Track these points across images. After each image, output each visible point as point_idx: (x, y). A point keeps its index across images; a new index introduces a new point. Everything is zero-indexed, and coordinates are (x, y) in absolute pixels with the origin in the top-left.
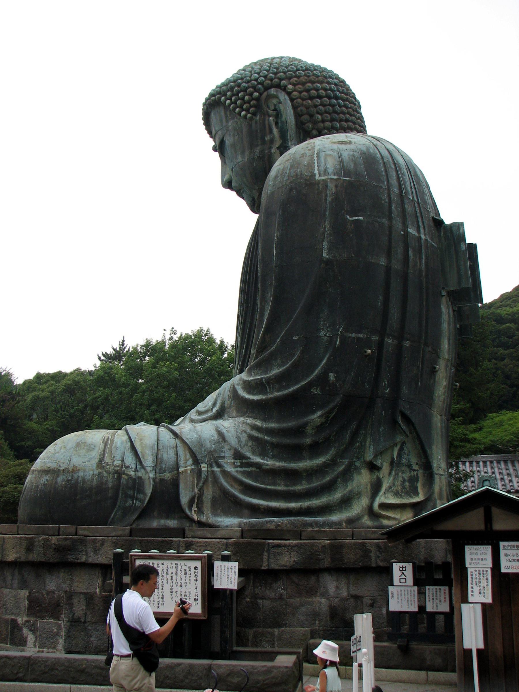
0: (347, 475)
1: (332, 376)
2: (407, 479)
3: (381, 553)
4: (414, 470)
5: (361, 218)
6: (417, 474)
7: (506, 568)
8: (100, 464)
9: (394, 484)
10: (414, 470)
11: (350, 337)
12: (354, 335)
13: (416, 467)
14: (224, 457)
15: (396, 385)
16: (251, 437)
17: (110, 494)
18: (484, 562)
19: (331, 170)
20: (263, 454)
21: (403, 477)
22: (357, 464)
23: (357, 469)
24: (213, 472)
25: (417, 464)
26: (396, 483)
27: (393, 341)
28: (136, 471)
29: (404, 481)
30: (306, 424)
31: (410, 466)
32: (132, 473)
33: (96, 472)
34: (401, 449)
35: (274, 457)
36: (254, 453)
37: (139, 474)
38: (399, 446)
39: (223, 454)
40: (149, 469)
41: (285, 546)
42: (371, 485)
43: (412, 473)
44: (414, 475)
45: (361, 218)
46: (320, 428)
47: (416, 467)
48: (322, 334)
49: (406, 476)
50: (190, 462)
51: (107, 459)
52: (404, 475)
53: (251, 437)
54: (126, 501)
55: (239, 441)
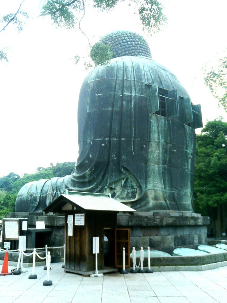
1: (91, 156)
5: (101, 94)
6: (136, 190)
7: (76, 223)
8: (28, 193)
10: (135, 189)
11: (96, 140)
12: (98, 139)
13: (135, 187)
14: (62, 188)
15: (119, 156)
16: (72, 180)
17: (29, 202)
18: (71, 221)
19: (92, 78)
20: (74, 186)
21: (128, 192)
22: (106, 187)
23: (105, 189)
24: (58, 193)
25: (136, 186)
26: (123, 194)
27: (116, 139)
28: (35, 194)
29: (128, 193)
30: (85, 174)
31: (132, 187)
32: (34, 195)
33: (26, 195)
34: (127, 180)
35: (78, 187)
36: (71, 186)
37: (36, 195)
38: (125, 180)
39: (62, 187)
40: (39, 193)
41: (61, 218)
43: (134, 190)
45: (101, 94)
46: (90, 175)
47: (135, 187)
48: (88, 140)
49: (130, 191)
50: (52, 190)
51: (30, 191)
52: (128, 191)
53: (72, 180)
54: (32, 204)
55: (68, 182)
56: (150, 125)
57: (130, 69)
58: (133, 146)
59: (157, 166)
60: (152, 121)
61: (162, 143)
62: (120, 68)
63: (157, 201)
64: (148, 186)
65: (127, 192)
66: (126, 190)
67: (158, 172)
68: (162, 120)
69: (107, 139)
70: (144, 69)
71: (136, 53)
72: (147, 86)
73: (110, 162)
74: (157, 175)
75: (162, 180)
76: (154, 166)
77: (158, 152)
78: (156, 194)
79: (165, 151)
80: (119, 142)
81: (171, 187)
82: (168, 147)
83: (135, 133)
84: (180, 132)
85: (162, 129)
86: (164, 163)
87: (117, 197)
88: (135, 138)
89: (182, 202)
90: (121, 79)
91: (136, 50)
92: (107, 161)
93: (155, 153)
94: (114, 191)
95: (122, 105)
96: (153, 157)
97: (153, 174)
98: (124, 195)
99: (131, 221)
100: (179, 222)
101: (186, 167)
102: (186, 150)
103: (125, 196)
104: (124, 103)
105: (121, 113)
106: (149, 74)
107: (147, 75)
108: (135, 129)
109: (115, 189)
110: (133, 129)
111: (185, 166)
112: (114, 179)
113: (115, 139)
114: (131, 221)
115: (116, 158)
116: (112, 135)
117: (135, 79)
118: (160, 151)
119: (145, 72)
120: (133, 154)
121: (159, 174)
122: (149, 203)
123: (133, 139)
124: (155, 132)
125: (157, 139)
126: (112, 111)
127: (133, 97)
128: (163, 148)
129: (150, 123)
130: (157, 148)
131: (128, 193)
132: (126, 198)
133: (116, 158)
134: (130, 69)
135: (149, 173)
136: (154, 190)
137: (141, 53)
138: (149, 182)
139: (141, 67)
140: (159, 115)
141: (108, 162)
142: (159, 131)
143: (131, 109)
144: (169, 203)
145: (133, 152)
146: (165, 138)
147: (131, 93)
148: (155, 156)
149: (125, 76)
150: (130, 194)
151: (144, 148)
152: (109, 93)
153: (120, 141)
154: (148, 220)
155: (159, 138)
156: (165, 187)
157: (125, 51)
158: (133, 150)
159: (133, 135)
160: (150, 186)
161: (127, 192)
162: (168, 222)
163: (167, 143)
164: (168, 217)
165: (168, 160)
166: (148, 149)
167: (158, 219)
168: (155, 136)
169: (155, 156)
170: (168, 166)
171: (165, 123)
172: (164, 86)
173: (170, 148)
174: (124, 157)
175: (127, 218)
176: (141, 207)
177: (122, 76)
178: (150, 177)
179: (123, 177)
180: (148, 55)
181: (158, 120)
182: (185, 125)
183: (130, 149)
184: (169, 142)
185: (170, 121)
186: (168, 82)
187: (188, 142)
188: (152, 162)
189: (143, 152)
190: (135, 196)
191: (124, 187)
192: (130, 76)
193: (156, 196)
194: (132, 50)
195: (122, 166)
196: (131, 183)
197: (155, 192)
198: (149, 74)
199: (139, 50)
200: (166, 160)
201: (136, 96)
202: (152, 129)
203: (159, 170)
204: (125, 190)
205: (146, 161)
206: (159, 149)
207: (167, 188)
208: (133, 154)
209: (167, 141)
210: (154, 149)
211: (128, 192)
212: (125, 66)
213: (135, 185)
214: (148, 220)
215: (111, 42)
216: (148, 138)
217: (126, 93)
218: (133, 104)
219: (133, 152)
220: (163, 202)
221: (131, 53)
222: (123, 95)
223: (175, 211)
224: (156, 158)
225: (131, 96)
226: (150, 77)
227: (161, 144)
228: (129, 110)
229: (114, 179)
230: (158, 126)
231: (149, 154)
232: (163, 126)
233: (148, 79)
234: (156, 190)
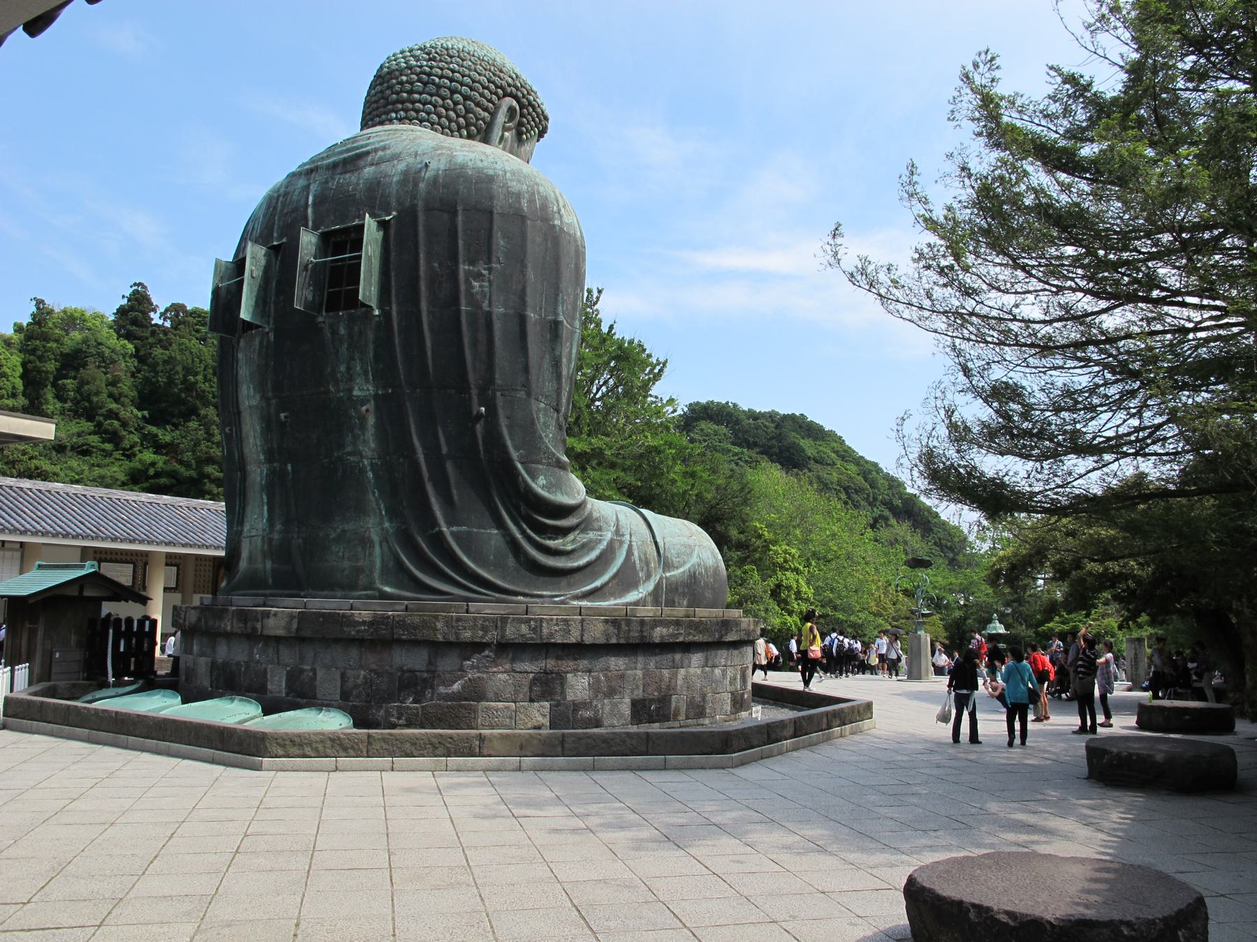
79: (269, 423)
82: (272, 410)
100: (206, 622)
101: (349, 449)
111: (341, 446)
144: (273, 570)
160: (246, 528)
163: (268, 399)
171: (261, 343)
207: (278, 527)
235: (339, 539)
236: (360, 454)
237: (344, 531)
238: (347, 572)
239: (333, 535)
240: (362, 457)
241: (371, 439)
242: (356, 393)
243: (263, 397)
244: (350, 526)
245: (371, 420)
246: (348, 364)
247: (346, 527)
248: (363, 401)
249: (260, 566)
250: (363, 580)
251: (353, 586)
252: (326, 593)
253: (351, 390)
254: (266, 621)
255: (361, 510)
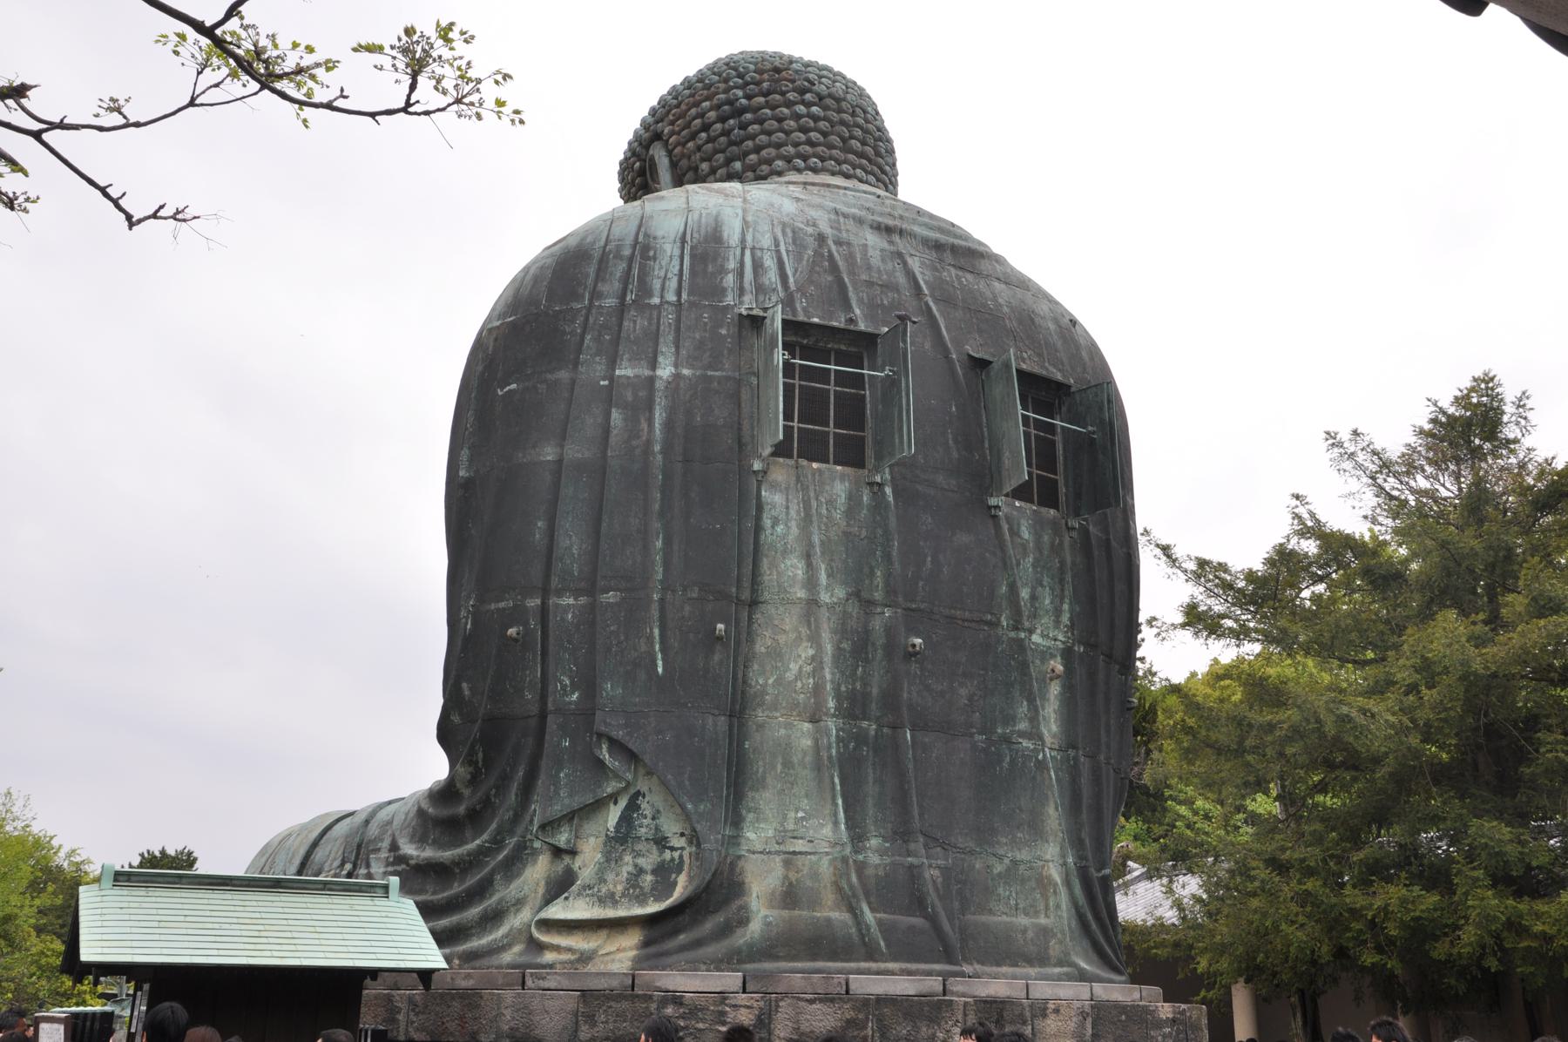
0: (513, 865)
2: (649, 868)
3: (417, 1014)
4: (672, 849)
5: (514, 386)
6: (681, 857)
9: (602, 881)
10: (672, 849)
15: (589, 686)
21: (636, 866)
23: (535, 853)
25: (682, 835)
26: (610, 877)
31: (661, 842)
34: (633, 806)
36: (412, 841)
38: (623, 803)
42: (547, 884)
43: (668, 855)
44: (673, 859)
45: (514, 386)
49: (647, 862)
52: (641, 861)
56: (758, 518)
57: (668, 247)
58: (656, 632)
59: (807, 726)
60: (773, 499)
61: (831, 607)
62: (619, 248)
63: (797, 912)
64: (750, 835)
65: (630, 868)
66: (628, 858)
67: (808, 759)
68: (838, 483)
69: (534, 602)
70: (743, 234)
71: (779, 163)
72: (747, 323)
73: (550, 718)
74: (806, 774)
75: (840, 802)
76: (788, 726)
77: (811, 652)
78: (793, 876)
79: (856, 648)
80: (590, 615)
81: (901, 834)
82: (877, 624)
83: (667, 564)
84: (963, 538)
85: (832, 534)
86: (853, 706)
87: (579, 895)
88: (666, 587)
89: (984, 918)
90: (610, 302)
91: (778, 146)
92: (534, 709)
93: (796, 658)
94: (567, 859)
95: (606, 430)
96: (779, 681)
97: (779, 767)
98: (616, 882)
99: (591, 1019)
101: (1023, 726)
102: (1013, 634)
103: (620, 888)
104: (616, 415)
105: (599, 470)
106: (769, 262)
107: (758, 266)
108: (668, 542)
109: (573, 853)
110: (659, 544)
111: (1010, 719)
112: (567, 801)
113: (571, 601)
114: (591, 1019)
115: (575, 697)
116: (555, 582)
117: (684, 296)
118: (819, 648)
119: (748, 253)
120: (660, 670)
121: (818, 767)
122: (744, 921)
123: (655, 597)
124: (785, 553)
125: (803, 587)
126: (560, 461)
127: (659, 385)
128: (842, 631)
129: (760, 508)
130: (804, 631)
131: (641, 871)
132: (623, 895)
133: (575, 697)
134: (670, 249)
135: (760, 767)
136: (778, 853)
137: (805, 158)
138: (756, 810)
139: (732, 233)
140: (815, 465)
141: (543, 716)
142: (810, 545)
143: (649, 443)
144: (880, 923)
145: (660, 663)
146: (856, 578)
147: (653, 365)
148: (790, 676)
149: (633, 285)
150: (649, 878)
151: (720, 638)
152: (549, 376)
153: (592, 607)
154: (682, 1017)
155: (811, 583)
156: (857, 837)
157: (728, 162)
158: (662, 651)
159: (660, 577)
160: (756, 835)
161: (630, 868)
162: (805, 1027)
163: (867, 605)
164: (811, 1002)
165: (875, 691)
166: (751, 639)
167: (743, 1010)
168: (787, 572)
169: (790, 676)
170: (880, 726)
171: (853, 498)
172: (858, 311)
173: (889, 631)
174: (610, 689)
175: (572, 1006)
176: (698, 943)
177: (617, 285)
178: (761, 784)
179: (609, 790)
180: (845, 167)
181: (805, 489)
182: (993, 501)
183: (643, 648)
184: (878, 596)
185: (888, 490)
186: (898, 291)
187: (1025, 593)
188: (775, 706)
189: (717, 657)
190: (675, 884)
191: (623, 836)
192: (657, 285)
193: (791, 884)
194: (758, 149)
195: (600, 735)
196: (653, 818)
197: (787, 864)
198: (769, 262)
199: (796, 145)
200: (866, 696)
201: (677, 376)
202: (767, 536)
203: (817, 748)
204: (621, 858)
205: (738, 706)
206: (815, 639)
207: (874, 842)
208: (660, 670)
209: (864, 595)
210: (782, 639)
211: (636, 866)
212: (641, 238)
213: (677, 828)
214: (682, 1017)
215: (672, 123)
216: (746, 584)
217: (624, 371)
218: (659, 416)
219: (660, 663)
220: (839, 916)
221: (753, 168)
222: (611, 379)
223: (913, 966)
224: (799, 684)
225: (651, 380)
226: (772, 276)
227: (824, 614)
228: (638, 451)
229: (565, 802)
230: (807, 520)
231: (756, 667)
232: (838, 515)
233: (760, 289)
234: (794, 853)
235: (1010, 875)
236: (1041, 738)
237: (1015, 862)
238: (1030, 934)
239: (999, 868)
240: (1043, 744)
241: (1053, 716)
242: (1036, 638)
243: (857, 594)
244: (1023, 855)
245: (1055, 689)
246: (1034, 589)
247: (1019, 857)
248: (1045, 655)
249: (839, 916)
250: (1055, 949)
251: (1042, 960)
252: (1004, 969)
253: (1031, 631)
254: (1039, 1023)
255: (1036, 830)
